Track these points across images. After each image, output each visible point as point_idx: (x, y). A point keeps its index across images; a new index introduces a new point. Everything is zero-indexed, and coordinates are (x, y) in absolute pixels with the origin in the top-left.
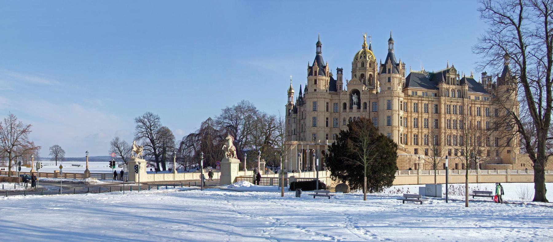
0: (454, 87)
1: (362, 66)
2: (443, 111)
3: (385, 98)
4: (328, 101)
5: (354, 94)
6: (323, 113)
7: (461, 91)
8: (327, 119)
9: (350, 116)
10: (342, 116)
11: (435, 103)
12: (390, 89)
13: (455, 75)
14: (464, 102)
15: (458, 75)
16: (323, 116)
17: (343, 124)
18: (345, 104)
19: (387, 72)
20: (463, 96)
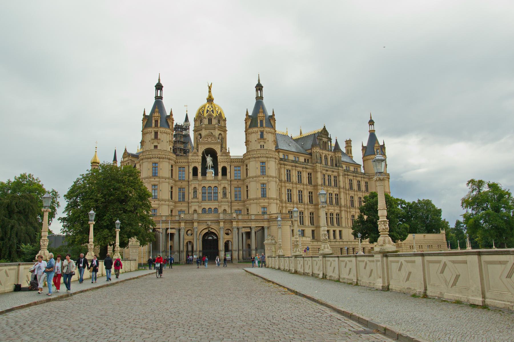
0: (327, 152)
1: (209, 123)
2: (320, 181)
3: (257, 159)
4: (173, 162)
5: (207, 156)
6: (167, 180)
7: (334, 158)
8: (172, 188)
9: (203, 185)
10: (191, 185)
11: (309, 171)
12: (263, 147)
13: (327, 138)
14: (338, 172)
15: (330, 139)
16: (168, 184)
17: (193, 197)
18: (195, 170)
19: (259, 124)
20: (336, 165)
